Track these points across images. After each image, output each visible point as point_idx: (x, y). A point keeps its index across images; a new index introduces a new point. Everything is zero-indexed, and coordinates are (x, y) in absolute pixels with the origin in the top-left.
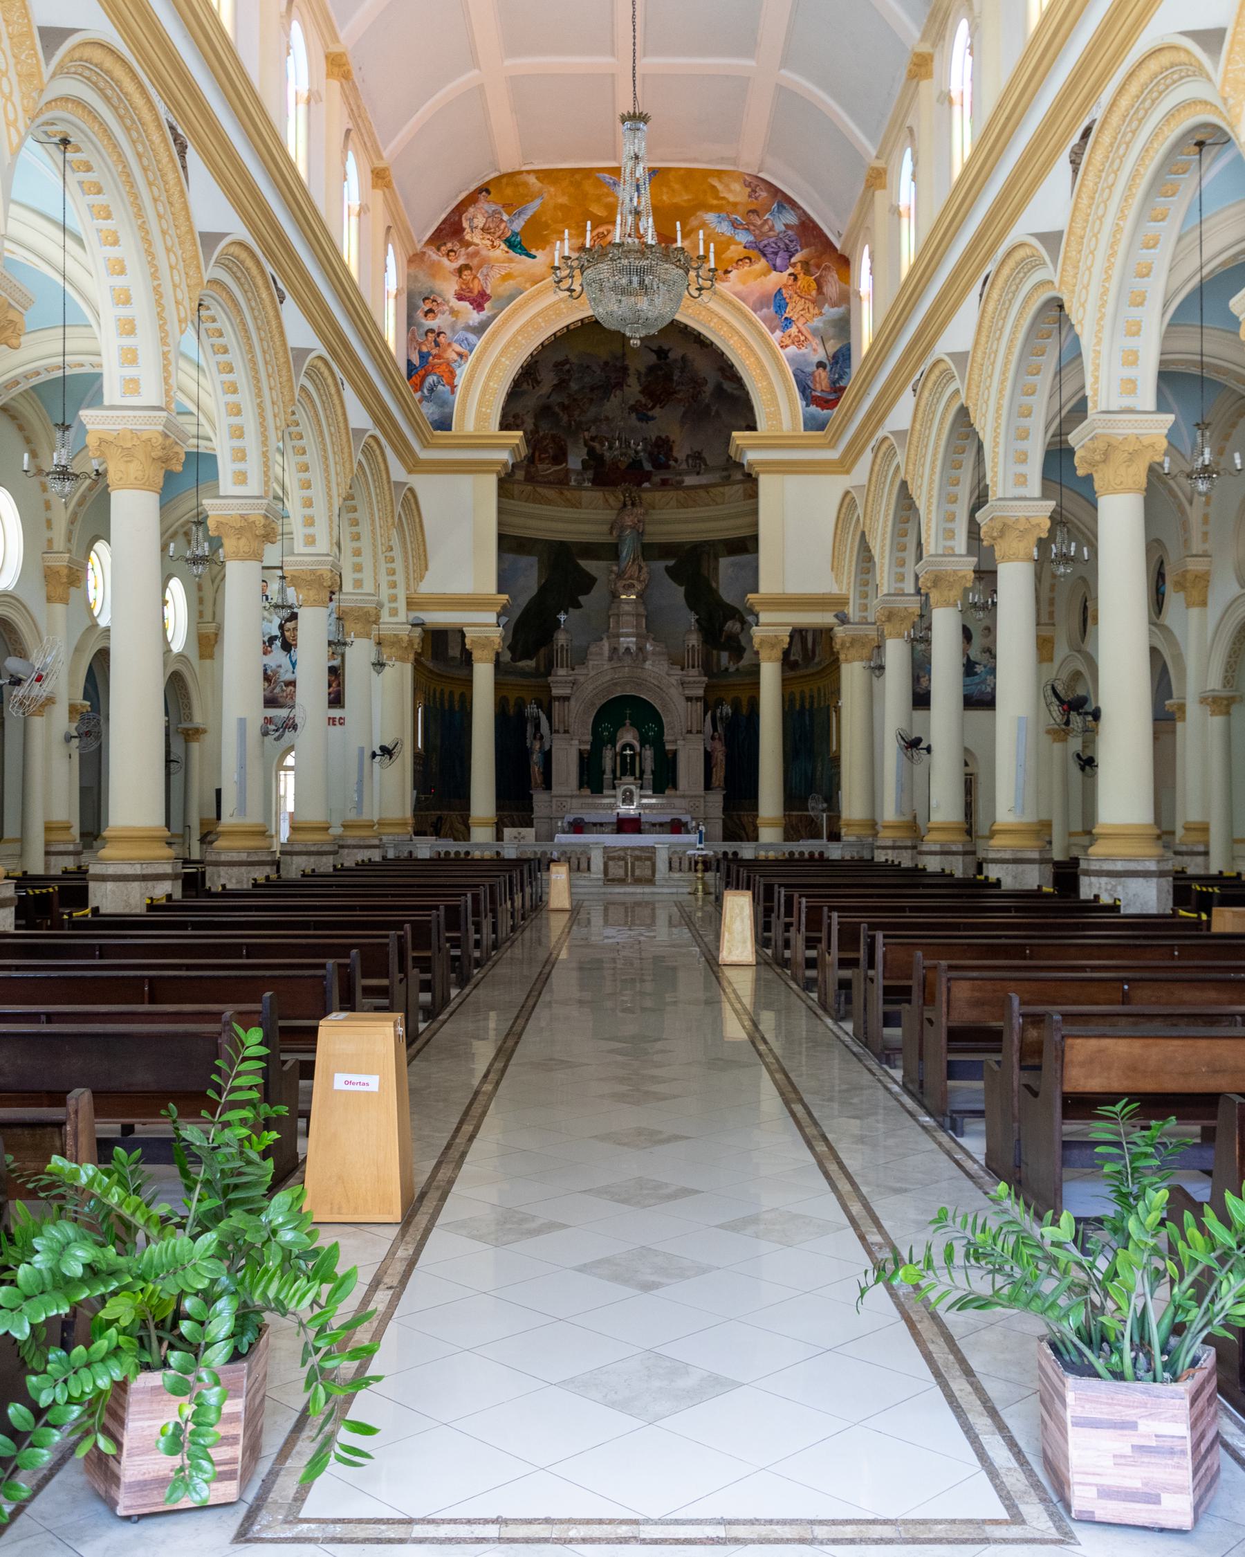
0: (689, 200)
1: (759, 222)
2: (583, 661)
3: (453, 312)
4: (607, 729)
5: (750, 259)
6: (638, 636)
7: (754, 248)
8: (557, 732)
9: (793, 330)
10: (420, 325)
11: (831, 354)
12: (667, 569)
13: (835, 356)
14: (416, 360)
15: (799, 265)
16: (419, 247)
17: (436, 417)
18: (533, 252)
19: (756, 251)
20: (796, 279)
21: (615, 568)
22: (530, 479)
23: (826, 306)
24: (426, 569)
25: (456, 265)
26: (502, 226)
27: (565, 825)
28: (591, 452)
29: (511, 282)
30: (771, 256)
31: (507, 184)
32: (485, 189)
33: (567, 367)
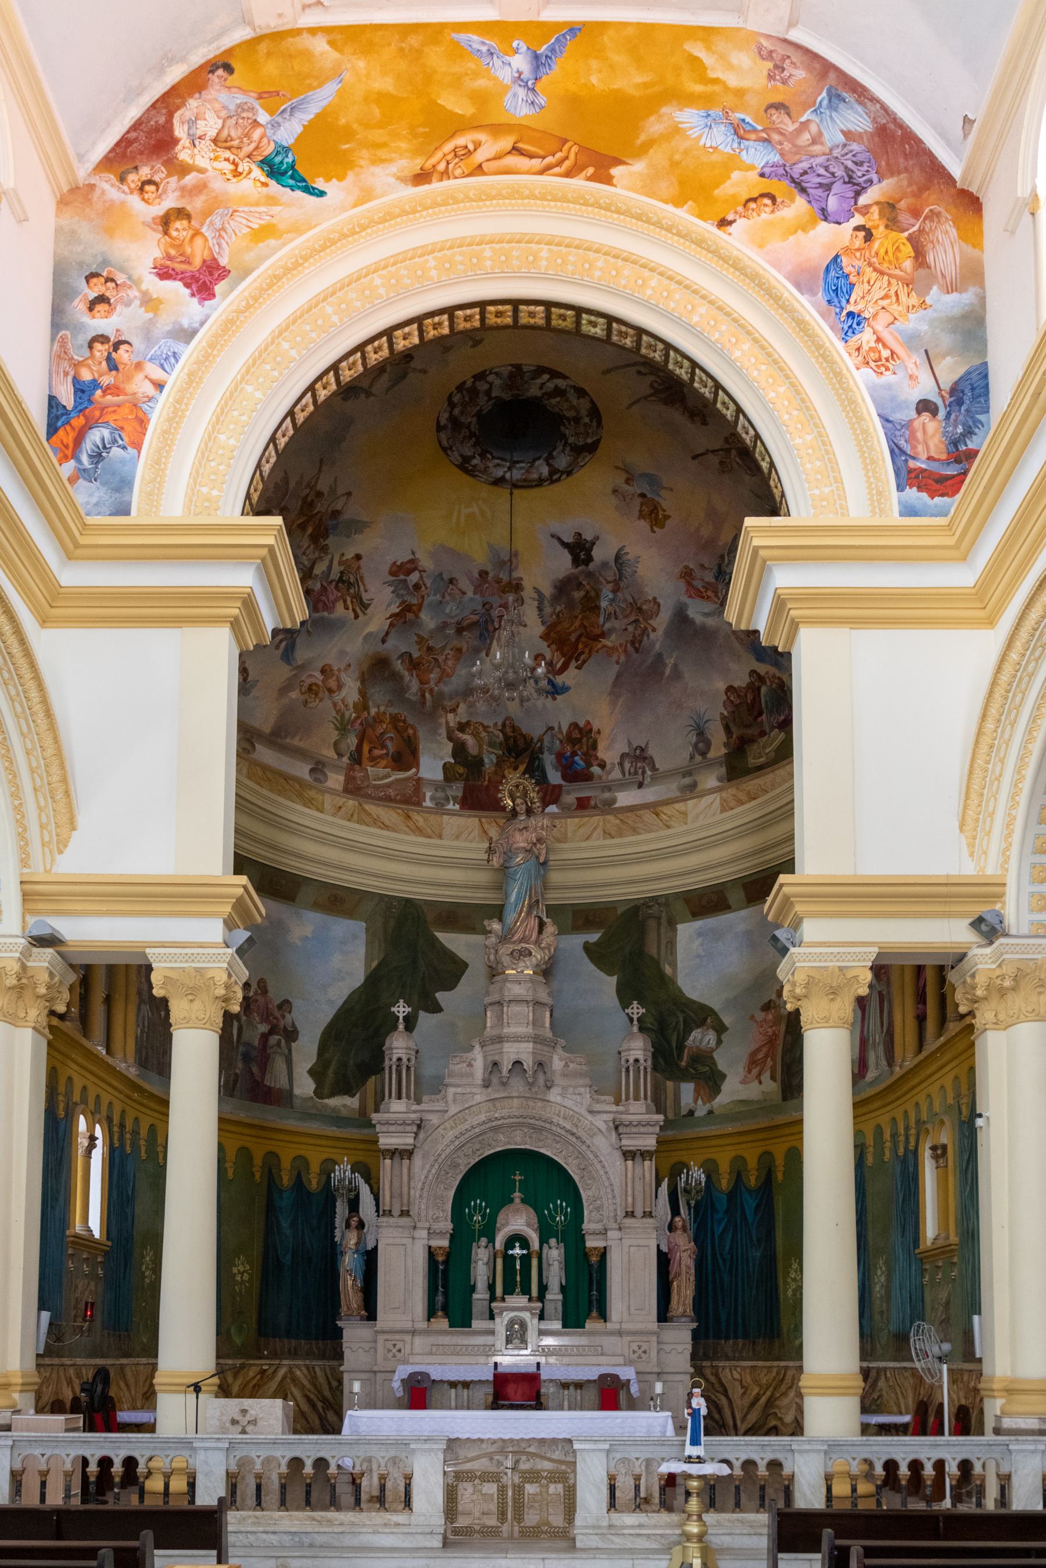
0: (645, 85)
1: (791, 127)
2: (437, 1086)
5: (773, 198)
6: (537, 1039)
12: (587, 948)
15: (875, 210)
16: (83, 172)
19: (785, 183)
22: (352, 789)
25: (159, 209)
26: (257, 134)
28: (459, 750)
30: (819, 192)
31: (269, 54)
32: (222, 64)
33: (414, 577)
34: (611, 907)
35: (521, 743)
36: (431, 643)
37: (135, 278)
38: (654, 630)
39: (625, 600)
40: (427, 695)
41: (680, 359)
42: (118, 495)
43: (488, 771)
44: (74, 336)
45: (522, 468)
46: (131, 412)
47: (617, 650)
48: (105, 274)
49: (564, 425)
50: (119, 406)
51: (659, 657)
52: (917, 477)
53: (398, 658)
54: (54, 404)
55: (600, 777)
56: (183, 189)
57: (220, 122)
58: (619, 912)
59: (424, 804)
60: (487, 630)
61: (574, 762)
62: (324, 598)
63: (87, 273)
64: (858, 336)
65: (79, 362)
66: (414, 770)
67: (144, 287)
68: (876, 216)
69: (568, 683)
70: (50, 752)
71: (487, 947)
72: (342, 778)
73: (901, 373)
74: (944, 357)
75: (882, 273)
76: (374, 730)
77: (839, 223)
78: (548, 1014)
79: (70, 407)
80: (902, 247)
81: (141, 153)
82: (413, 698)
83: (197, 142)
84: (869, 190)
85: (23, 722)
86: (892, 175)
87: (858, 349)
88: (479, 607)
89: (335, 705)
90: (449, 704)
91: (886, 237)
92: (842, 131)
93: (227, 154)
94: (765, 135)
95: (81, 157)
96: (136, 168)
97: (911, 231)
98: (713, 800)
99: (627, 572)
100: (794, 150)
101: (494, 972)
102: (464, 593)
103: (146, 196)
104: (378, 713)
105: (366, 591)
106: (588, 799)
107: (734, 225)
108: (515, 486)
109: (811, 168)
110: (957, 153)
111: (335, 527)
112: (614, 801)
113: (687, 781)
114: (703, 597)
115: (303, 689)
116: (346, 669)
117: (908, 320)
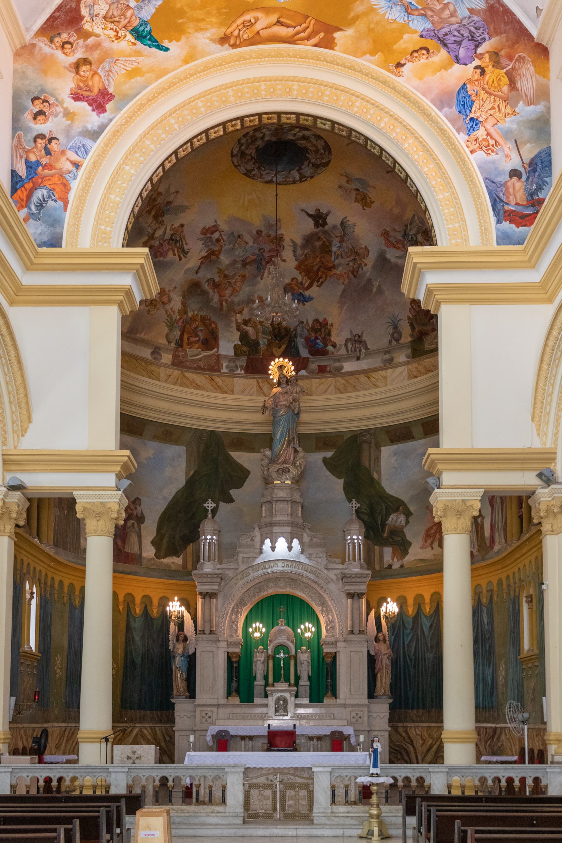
1: (438, 7)
3: (68, 114)
4: (259, 630)
5: (427, 50)
7: (431, 37)
8: (203, 632)
9: (481, 133)
10: (28, 130)
11: (527, 160)
12: (325, 461)
13: (531, 164)
14: (22, 171)
15: (487, 56)
16: (28, 37)
17: (45, 238)
18: (166, 44)
20: (483, 72)
21: (268, 453)
22: (177, 363)
23: (521, 103)
24: (30, 421)
25: (73, 59)
27: (209, 738)
28: (244, 337)
29: (139, 78)
30: (454, 46)
33: (216, 235)
34: (339, 435)
35: (283, 332)
36: (226, 273)
37: (60, 100)
38: (366, 265)
39: (348, 247)
40: (224, 303)
41: (373, 145)
42: (52, 229)
43: (262, 349)
44: (25, 135)
45: (282, 175)
46: (59, 180)
47: (343, 276)
48: (42, 97)
49: (308, 153)
50: (52, 176)
51: (369, 281)
52: (509, 215)
53: (206, 282)
54: (14, 175)
55: (333, 353)
56: (87, 47)
57: (107, 6)
58: (345, 438)
59: (222, 371)
60: (262, 265)
61: (316, 343)
62: (160, 250)
63: (32, 97)
64: (476, 132)
65: (29, 150)
66: (215, 350)
67: (65, 105)
68: (487, 60)
69: (313, 295)
70: (19, 381)
71: (262, 466)
72: (170, 356)
73: (501, 154)
74: (526, 144)
75: (490, 94)
76: (190, 326)
77: (466, 65)
78: (300, 508)
79: (24, 177)
80: (502, 78)
81: (62, 25)
82: (216, 306)
83: (94, 19)
84: (483, 44)
85: (6, 368)
86: (497, 35)
87: (476, 140)
88: (257, 251)
89: (166, 312)
90: (237, 308)
91: (493, 72)
92: (468, 9)
93: (112, 26)
94: (423, 12)
95: (28, 30)
96: (59, 34)
97: (507, 69)
98: (403, 370)
99: (349, 231)
100: (440, 20)
101: (267, 481)
102: (247, 243)
103: (66, 51)
104: (193, 316)
105: (186, 244)
106: (325, 366)
107: (405, 66)
108: (278, 184)
109: (450, 31)
110: (535, 23)
111: (168, 211)
112: (342, 368)
113: (387, 356)
114: (395, 247)
115: (147, 303)
116: (173, 290)
117: (505, 122)
